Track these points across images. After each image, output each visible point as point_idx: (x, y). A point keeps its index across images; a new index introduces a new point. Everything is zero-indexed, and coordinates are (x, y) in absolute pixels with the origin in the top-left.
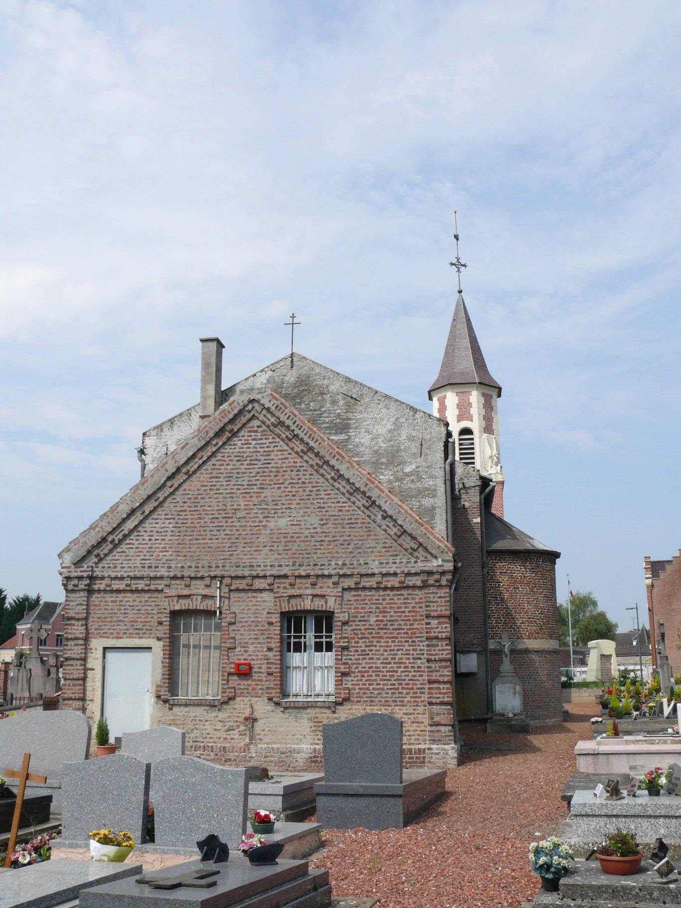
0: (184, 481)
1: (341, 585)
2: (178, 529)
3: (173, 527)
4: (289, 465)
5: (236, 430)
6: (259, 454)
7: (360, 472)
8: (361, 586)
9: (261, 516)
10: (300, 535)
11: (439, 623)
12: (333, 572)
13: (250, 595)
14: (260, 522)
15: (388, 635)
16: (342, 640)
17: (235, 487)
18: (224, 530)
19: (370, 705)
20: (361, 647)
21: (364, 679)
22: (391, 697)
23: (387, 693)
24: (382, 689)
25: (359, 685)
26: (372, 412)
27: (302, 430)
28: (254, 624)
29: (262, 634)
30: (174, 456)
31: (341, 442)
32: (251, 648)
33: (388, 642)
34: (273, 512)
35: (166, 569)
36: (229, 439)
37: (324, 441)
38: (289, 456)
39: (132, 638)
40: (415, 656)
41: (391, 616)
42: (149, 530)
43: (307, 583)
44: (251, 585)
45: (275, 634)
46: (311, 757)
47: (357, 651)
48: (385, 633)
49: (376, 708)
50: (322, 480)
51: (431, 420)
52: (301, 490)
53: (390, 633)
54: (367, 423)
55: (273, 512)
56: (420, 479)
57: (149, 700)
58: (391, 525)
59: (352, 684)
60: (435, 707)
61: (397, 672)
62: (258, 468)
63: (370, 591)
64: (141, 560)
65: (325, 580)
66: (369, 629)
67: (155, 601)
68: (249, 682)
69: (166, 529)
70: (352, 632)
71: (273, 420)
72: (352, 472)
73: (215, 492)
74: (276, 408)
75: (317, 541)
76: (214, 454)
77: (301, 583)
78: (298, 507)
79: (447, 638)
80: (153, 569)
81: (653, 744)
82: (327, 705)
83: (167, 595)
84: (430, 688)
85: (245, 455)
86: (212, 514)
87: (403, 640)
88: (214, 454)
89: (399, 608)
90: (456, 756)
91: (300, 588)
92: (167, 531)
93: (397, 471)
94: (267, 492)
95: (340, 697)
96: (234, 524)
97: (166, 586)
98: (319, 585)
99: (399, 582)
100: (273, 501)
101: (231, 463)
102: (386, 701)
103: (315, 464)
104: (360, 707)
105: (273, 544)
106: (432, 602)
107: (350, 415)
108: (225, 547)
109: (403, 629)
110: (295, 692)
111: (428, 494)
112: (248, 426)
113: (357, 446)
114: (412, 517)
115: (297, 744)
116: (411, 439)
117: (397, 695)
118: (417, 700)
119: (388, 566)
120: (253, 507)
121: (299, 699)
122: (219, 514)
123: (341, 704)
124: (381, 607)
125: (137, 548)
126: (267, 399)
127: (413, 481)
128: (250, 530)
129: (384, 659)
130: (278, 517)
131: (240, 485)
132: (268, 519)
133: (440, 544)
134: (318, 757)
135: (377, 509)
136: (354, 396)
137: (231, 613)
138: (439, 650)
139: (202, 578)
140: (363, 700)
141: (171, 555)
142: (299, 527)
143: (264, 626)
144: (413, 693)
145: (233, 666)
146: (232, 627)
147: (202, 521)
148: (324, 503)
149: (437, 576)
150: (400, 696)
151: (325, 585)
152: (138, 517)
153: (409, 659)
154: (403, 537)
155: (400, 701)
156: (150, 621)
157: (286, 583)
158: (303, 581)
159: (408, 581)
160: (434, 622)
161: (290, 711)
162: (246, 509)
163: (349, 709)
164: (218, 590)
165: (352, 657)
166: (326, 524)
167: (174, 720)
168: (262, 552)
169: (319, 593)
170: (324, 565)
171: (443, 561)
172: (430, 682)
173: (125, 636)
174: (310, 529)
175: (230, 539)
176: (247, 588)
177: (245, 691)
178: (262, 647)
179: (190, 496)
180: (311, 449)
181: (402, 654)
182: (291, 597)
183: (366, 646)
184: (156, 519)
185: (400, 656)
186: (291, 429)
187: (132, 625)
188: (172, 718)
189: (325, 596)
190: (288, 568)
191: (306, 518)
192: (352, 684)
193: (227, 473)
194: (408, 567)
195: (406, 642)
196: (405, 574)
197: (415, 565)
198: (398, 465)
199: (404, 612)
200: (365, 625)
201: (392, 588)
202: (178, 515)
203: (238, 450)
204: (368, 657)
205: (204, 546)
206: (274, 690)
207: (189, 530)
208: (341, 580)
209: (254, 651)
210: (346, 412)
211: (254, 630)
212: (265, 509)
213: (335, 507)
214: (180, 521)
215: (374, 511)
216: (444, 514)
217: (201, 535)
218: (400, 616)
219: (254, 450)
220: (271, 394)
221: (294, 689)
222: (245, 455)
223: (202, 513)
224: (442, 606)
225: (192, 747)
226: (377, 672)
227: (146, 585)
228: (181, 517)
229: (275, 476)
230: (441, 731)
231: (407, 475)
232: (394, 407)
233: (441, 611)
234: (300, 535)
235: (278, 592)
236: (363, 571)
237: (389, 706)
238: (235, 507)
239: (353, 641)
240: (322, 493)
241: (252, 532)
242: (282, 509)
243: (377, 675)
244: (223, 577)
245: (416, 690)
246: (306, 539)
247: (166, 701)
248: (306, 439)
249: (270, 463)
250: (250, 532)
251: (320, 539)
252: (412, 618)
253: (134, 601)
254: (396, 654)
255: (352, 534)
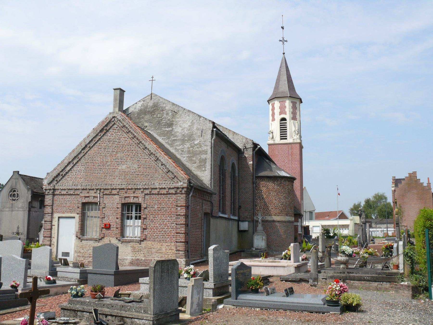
0: (88, 150)
1: (144, 192)
2: (86, 170)
3: (84, 169)
4: (127, 143)
5: (108, 129)
6: (116, 139)
7: (153, 146)
8: (152, 193)
9: (116, 164)
10: (130, 172)
11: (181, 209)
12: (141, 187)
13: (111, 196)
14: (116, 167)
15: (161, 213)
16: (144, 215)
17: (107, 153)
18: (102, 170)
19: (154, 242)
20: (151, 218)
21: (152, 231)
22: (162, 239)
23: (160, 237)
24: (158, 235)
25: (150, 233)
26: (182, 118)
27: (132, 129)
28: (112, 208)
29: (115, 212)
30: (84, 140)
31: (169, 131)
32: (111, 218)
33: (161, 216)
34: (120, 162)
35: (80, 186)
36: (105, 133)
37: (140, 133)
38: (127, 140)
39: (68, 213)
40: (172, 222)
41: (163, 206)
42: (75, 170)
43: (132, 192)
44: (111, 192)
45: (119, 212)
46: (131, 262)
47: (149, 220)
48: (161, 213)
49: (156, 243)
50: (139, 149)
51: (206, 121)
52: (131, 153)
53: (162, 213)
54: (180, 122)
55: (120, 162)
56: (201, 146)
57: (74, 237)
58: (164, 168)
59: (147, 233)
60: (178, 243)
61: (164, 228)
62: (116, 145)
63: (155, 195)
64: (72, 182)
65: (138, 190)
66: (154, 211)
67: (77, 199)
68: (110, 231)
69: (81, 170)
70: (148, 212)
71: (121, 125)
72: (150, 146)
73: (100, 154)
74: (123, 120)
75: (136, 175)
76: (100, 139)
77: (129, 192)
78: (130, 160)
79: (183, 215)
80: (76, 186)
81: (261, 262)
82: (137, 241)
83: (81, 196)
84: (176, 236)
85: (111, 139)
86: (98, 164)
87: (167, 215)
88: (100, 139)
89: (166, 202)
90: (185, 263)
91: (129, 194)
92: (82, 171)
93: (192, 143)
94: (119, 155)
95: (142, 238)
96: (106, 168)
97: (80, 192)
98: (136, 192)
99: (166, 192)
100: (121, 158)
101: (106, 143)
102: (160, 240)
103: (136, 143)
104: (150, 242)
105: (120, 176)
106: (179, 200)
107: (174, 119)
108: (102, 177)
109: (167, 211)
110: (127, 236)
111: (204, 153)
112: (113, 127)
113: (176, 133)
114: (172, 164)
115: (126, 256)
116: (198, 129)
117: (164, 238)
118: (172, 240)
119: (162, 185)
120: (113, 161)
121: (129, 238)
122: (101, 164)
123: (143, 241)
124: (159, 202)
125: (71, 177)
126: (119, 116)
127: (198, 147)
128: (112, 170)
129: (160, 223)
130: (122, 165)
131: (109, 152)
132: (119, 165)
133: (183, 176)
134: (133, 262)
135: (159, 161)
136: (175, 111)
137: (104, 204)
138: (180, 220)
139: (93, 189)
140: (151, 239)
141: (83, 180)
142: (130, 169)
143: (115, 209)
144: (170, 237)
145: (104, 225)
146: (104, 209)
147: (95, 166)
148: (139, 159)
149: (180, 189)
150: (165, 238)
151: (138, 193)
152: (71, 165)
153: (169, 223)
154: (169, 173)
155: (165, 241)
156: (75, 207)
157: (123, 191)
158: (130, 191)
159: (170, 191)
160: (179, 208)
161: (124, 243)
162: (110, 162)
163: (146, 243)
164: (99, 194)
165: (148, 222)
166: (140, 167)
167: (82, 246)
168: (116, 179)
169: (136, 196)
170: (138, 184)
171: (183, 183)
172: (177, 233)
173: (66, 212)
174: (134, 169)
175: (104, 174)
176: (110, 193)
177: (108, 235)
178: (114, 217)
179: (90, 157)
180: (135, 137)
181: (167, 221)
182: (125, 197)
183: (153, 218)
184: (78, 166)
185: (166, 222)
186: (128, 128)
187: (68, 208)
188: (81, 245)
189: (138, 197)
190: (124, 185)
191: (133, 165)
192: (147, 233)
193: (104, 147)
194: (169, 185)
195: (168, 216)
196: (169, 188)
197: (172, 184)
198: (192, 141)
199: (168, 204)
200: (153, 209)
201: (164, 194)
202: (86, 164)
203: (109, 137)
204: (153, 222)
205: (95, 176)
206: (118, 235)
207: (90, 170)
208: (144, 190)
209: (112, 219)
210: (172, 118)
211: (112, 211)
212: (118, 161)
213: (144, 160)
214: (86, 167)
215: (158, 162)
216: (210, 162)
217: (94, 172)
218: (167, 206)
219: (115, 137)
220: (121, 114)
221: (127, 234)
222: (111, 139)
223: (95, 163)
224: (182, 202)
225: (88, 256)
226: (157, 228)
227: (73, 192)
228: (87, 165)
229: (122, 148)
230: (180, 253)
231: (196, 145)
232: (192, 116)
233: (182, 204)
234: (130, 172)
235: (120, 195)
236: (153, 187)
237: (161, 242)
238: (107, 161)
239: (148, 215)
240: (139, 155)
241: (113, 171)
242: (124, 161)
243: (157, 230)
244: (101, 189)
245: (171, 236)
246: (132, 174)
247: (79, 238)
248: (133, 132)
249: (120, 143)
250: (112, 171)
251: (137, 174)
252: (171, 207)
253: (69, 198)
254: (164, 221)
255: (150, 171)
